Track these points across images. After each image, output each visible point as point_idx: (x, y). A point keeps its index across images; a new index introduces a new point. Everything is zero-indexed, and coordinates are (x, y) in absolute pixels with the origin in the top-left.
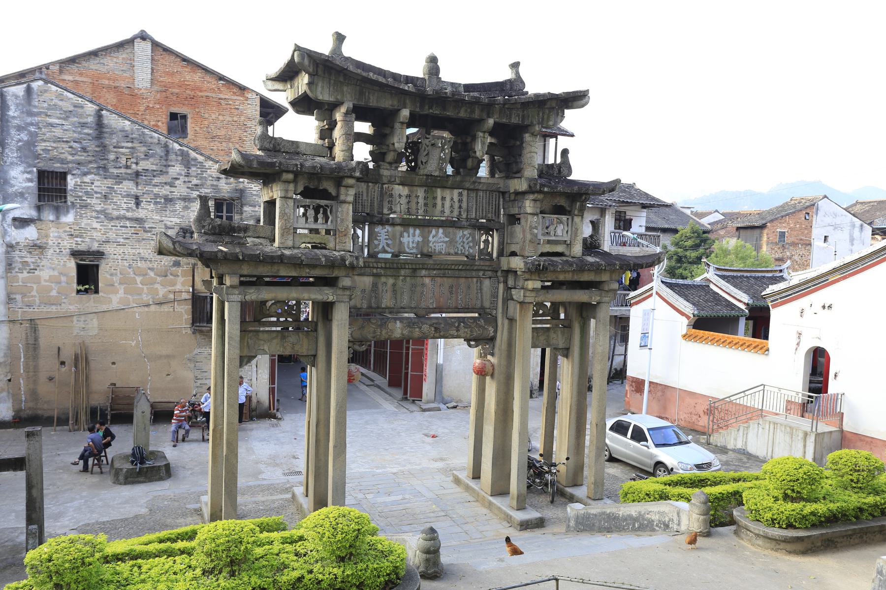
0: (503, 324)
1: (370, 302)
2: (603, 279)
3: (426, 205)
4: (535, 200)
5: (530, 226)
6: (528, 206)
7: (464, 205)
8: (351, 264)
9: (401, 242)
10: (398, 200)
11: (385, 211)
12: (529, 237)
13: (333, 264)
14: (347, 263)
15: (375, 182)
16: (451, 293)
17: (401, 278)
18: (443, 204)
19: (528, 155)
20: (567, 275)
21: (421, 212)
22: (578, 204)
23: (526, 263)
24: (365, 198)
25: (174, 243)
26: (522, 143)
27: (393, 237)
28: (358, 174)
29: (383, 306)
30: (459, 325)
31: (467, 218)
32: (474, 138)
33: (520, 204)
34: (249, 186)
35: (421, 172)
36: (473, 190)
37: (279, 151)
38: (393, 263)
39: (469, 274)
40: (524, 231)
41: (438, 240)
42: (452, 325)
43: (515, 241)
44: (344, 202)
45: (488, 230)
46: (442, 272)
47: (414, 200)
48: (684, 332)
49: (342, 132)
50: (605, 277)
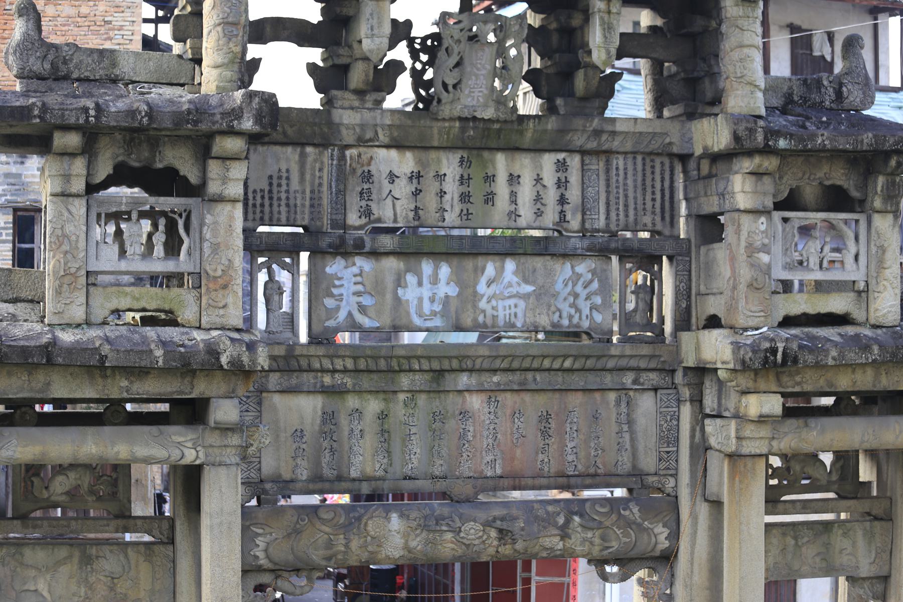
0: (694, 516)
1: (318, 463)
3: (465, 198)
4: (757, 174)
6: (741, 189)
7: (574, 194)
9: (397, 300)
11: (353, 219)
12: (745, 274)
13: (185, 365)
14: (224, 360)
15: (324, 145)
16: (545, 433)
17: (402, 397)
19: (736, 55)
21: (451, 217)
22: (881, 180)
23: (737, 346)
24: (295, 185)
28: (248, 124)
29: (354, 474)
30: (568, 521)
31: (583, 230)
35: (446, 111)
36: (596, 153)
38: (375, 358)
39: (592, 380)
40: (733, 259)
41: (504, 291)
42: (549, 520)
44: (219, 199)
45: (648, 260)
46: (517, 377)
47: (430, 187)
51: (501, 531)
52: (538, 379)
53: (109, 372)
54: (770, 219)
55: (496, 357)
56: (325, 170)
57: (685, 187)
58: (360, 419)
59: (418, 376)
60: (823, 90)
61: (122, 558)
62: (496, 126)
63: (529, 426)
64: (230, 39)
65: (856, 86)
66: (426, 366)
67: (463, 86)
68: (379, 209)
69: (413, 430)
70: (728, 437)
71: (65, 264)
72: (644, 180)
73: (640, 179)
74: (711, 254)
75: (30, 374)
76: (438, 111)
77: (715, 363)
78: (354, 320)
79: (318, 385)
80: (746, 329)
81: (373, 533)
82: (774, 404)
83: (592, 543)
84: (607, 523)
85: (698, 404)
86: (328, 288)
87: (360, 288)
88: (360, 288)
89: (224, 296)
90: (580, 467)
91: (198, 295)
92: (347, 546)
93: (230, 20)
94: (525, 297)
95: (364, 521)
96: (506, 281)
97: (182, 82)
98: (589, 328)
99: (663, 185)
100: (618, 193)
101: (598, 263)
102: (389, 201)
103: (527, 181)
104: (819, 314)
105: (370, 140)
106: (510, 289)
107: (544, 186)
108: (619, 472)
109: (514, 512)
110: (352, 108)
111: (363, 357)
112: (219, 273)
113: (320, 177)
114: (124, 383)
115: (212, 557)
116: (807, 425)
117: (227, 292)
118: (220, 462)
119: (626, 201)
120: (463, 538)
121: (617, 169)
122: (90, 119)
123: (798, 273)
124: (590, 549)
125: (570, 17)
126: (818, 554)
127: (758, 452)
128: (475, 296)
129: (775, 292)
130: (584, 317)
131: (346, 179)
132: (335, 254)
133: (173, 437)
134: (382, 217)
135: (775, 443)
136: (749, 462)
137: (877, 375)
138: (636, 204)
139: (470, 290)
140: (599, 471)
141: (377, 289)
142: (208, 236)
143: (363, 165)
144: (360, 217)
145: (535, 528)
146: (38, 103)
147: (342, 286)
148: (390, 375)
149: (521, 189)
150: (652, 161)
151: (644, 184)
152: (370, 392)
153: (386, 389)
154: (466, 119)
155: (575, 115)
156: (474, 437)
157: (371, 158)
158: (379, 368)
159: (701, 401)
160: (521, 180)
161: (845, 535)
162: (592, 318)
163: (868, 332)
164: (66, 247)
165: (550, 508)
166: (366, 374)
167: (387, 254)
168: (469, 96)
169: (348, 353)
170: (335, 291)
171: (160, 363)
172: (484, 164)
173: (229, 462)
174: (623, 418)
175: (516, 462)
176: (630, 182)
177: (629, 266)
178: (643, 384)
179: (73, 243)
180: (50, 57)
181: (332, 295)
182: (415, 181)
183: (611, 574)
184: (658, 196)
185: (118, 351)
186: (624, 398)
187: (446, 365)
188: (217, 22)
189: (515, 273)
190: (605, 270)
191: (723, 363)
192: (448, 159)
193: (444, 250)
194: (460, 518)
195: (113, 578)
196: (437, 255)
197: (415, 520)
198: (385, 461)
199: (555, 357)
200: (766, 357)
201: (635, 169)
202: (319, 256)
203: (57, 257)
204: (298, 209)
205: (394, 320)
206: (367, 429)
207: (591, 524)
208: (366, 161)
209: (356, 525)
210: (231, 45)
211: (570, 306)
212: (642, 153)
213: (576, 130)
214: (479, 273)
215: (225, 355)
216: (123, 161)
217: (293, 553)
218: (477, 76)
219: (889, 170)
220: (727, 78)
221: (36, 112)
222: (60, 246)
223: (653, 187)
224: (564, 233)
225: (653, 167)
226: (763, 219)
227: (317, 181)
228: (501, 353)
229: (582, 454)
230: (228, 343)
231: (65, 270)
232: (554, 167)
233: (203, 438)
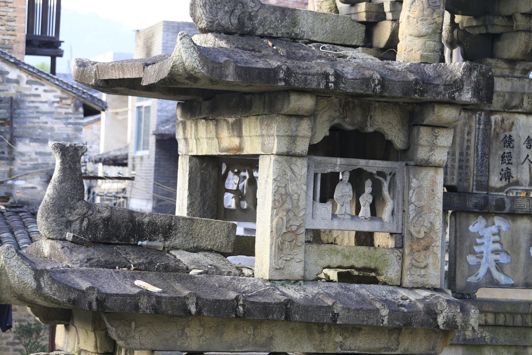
8: (451, 325)
11: (495, 181)
14: (440, 320)
25: (38, 274)
28: (467, 96)
34: (33, 89)
37: (251, 34)
44: (426, 164)
53: (326, 328)
56: (473, 134)
64: (434, 10)
68: (517, 172)
71: (288, 221)
75: (255, 328)
78: (492, 277)
79: (461, 338)
86: (471, 246)
87: (497, 246)
88: (497, 246)
89: (425, 257)
91: (400, 255)
97: (354, 44)
105: (516, 107)
110: (504, 76)
111: (503, 313)
112: (422, 235)
113: (468, 141)
117: (428, 253)
122: (330, 84)
131: (491, 143)
132: (477, 214)
134: (520, 180)
142: (413, 199)
143: (505, 131)
144: (501, 179)
146: (283, 67)
147: (482, 244)
152: (504, 346)
153: (519, 343)
157: (513, 123)
158: (515, 324)
164: (288, 206)
166: (502, 329)
167: (523, 215)
169: (491, 309)
170: (477, 249)
171: (385, 322)
179: (295, 202)
180: (237, 12)
181: (473, 253)
185: (349, 309)
202: (464, 215)
203: (280, 215)
204: (448, 169)
205: (526, 278)
210: (435, 16)
215: (442, 316)
216: (339, 124)
221: (282, 76)
222: (283, 204)
227: (465, 144)
230: (445, 304)
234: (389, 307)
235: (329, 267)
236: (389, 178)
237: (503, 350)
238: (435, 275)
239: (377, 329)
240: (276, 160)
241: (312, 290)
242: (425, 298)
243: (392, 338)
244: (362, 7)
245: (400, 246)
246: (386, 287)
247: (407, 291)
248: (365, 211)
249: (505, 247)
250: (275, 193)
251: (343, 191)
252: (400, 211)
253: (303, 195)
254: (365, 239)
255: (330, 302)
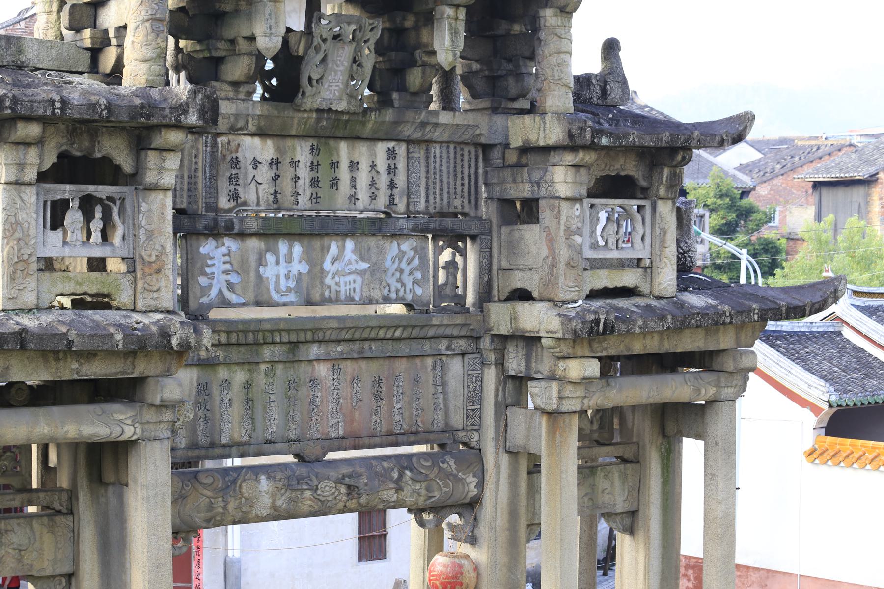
0: (497, 466)
1: (194, 432)
2: (722, 347)
3: (315, 183)
5: (568, 228)
6: (562, 179)
7: (401, 180)
8: (185, 347)
9: (259, 277)
10: (251, 172)
11: (224, 202)
12: (564, 254)
13: (139, 346)
14: (174, 342)
16: (377, 397)
17: (263, 367)
18: (353, 179)
19: (553, 60)
20: (648, 341)
21: (304, 201)
22: (666, 171)
23: (566, 319)
26: (536, 30)
27: (242, 268)
28: (193, 119)
29: (224, 440)
30: (401, 475)
31: (408, 212)
32: (428, 19)
33: (536, 175)
36: (418, 142)
39: (415, 348)
40: (551, 241)
42: (384, 476)
43: (521, 263)
46: (356, 346)
47: (287, 173)
48: (808, 446)
49: (144, 15)
50: (725, 340)
51: (349, 487)
52: (373, 347)
54: (581, 205)
55: (343, 329)
56: (200, 157)
57: (486, 173)
58: (229, 389)
59: (277, 348)
60: (592, 88)
61: (28, 531)
62: (346, 117)
63: (365, 390)
64: (158, 35)
65: (617, 84)
66: (285, 340)
67: (324, 80)
68: (245, 193)
69: (273, 398)
70: (550, 397)
71: (19, 251)
72: (455, 167)
73: (452, 166)
74: (516, 234)
76: (301, 103)
77: (538, 332)
78: (224, 298)
79: (196, 358)
80: (564, 303)
81: (246, 495)
82: (593, 368)
83: (419, 494)
84: (432, 476)
85: (500, 366)
86: (202, 268)
87: (228, 266)
88: (228, 266)
89: (157, 280)
90: (405, 426)
92: (225, 508)
93: (158, 16)
94: (361, 273)
95: (238, 484)
96: (346, 259)
97: (80, 70)
98: (412, 300)
99: (469, 172)
100: (435, 178)
101: (419, 242)
102: (253, 185)
103: (364, 168)
104: (616, 288)
105: (241, 129)
106: (350, 267)
107: (378, 172)
108: (435, 429)
109: (359, 469)
110: (228, 99)
111: (235, 332)
112: (153, 258)
113: (196, 163)
114: (75, 365)
115: (149, 527)
116: (608, 385)
117: (160, 276)
118: (155, 437)
119: (441, 186)
120: (319, 495)
121: (435, 156)
123: (601, 252)
124: (417, 500)
125: (404, 19)
126: (586, 495)
127: (574, 409)
128: (322, 273)
129: (585, 270)
130: (408, 291)
131: (218, 165)
132: (207, 236)
133: (115, 415)
135: (586, 401)
136: (567, 418)
137: (661, 339)
138: (449, 188)
139: (318, 268)
140: (420, 429)
141: (242, 268)
142: (143, 223)
143: (231, 152)
145: (376, 483)
146: (9, 95)
147: (213, 265)
148: (255, 348)
149: (359, 174)
150: (462, 149)
151: (455, 171)
152: (238, 364)
153: (251, 360)
154: (323, 111)
155: (408, 107)
156: (321, 402)
159: (503, 364)
160: (360, 167)
161: (606, 476)
162: (414, 292)
163: (654, 303)
164: (18, 234)
165: (385, 464)
166: (235, 347)
168: (327, 90)
169: (223, 329)
170: (208, 270)
171: (120, 347)
172: (330, 152)
173: (162, 437)
174: (438, 380)
175: (355, 424)
176: (444, 168)
177: (441, 243)
178: (454, 350)
179: (25, 230)
181: (205, 274)
182: (274, 167)
183: (428, 521)
184: (466, 181)
186: (438, 363)
187: (302, 337)
188: (146, 18)
189: (354, 251)
190: (424, 248)
191: (547, 332)
192: (301, 147)
193: (299, 232)
194: (317, 477)
195: (20, 550)
196: (292, 236)
197: (280, 480)
198: (250, 427)
199: (389, 328)
200: (592, 328)
201: (448, 157)
202: (194, 237)
203: (11, 244)
205: (256, 297)
206: (235, 398)
207: (420, 477)
208: (234, 148)
209: (233, 487)
210: (159, 40)
211: (397, 281)
212: (454, 143)
213: (408, 122)
214: (325, 251)
216: (66, 151)
217: (179, 517)
218: (336, 71)
219: (674, 163)
220: (545, 80)
221: (8, 103)
222: (14, 233)
223: (462, 173)
224: (393, 215)
225: (462, 155)
226: (577, 206)
228: (348, 326)
229: (406, 414)
230: (178, 326)
231: (18, 257)
232: (385, 155)
233: (141, 415)
234: (123, 331)
235: (62, 295)
236: (118, 203)
237: (236, 368)
238: (168, 297)
239: (112, 354)
240: (5, 189)
241: (46, 318)
242: (159, 321)
243: (128, 362)
244: (87, 33)
245: (132, 271)
246: (119, 312)
247: (140, 314)
248: (96, 236)
249: (235, 267)
250: (5, 223)
251: (74, 217)
252: (131, 235)
253: (33, 223)
254: (97, 265)
255: (64, 329)
